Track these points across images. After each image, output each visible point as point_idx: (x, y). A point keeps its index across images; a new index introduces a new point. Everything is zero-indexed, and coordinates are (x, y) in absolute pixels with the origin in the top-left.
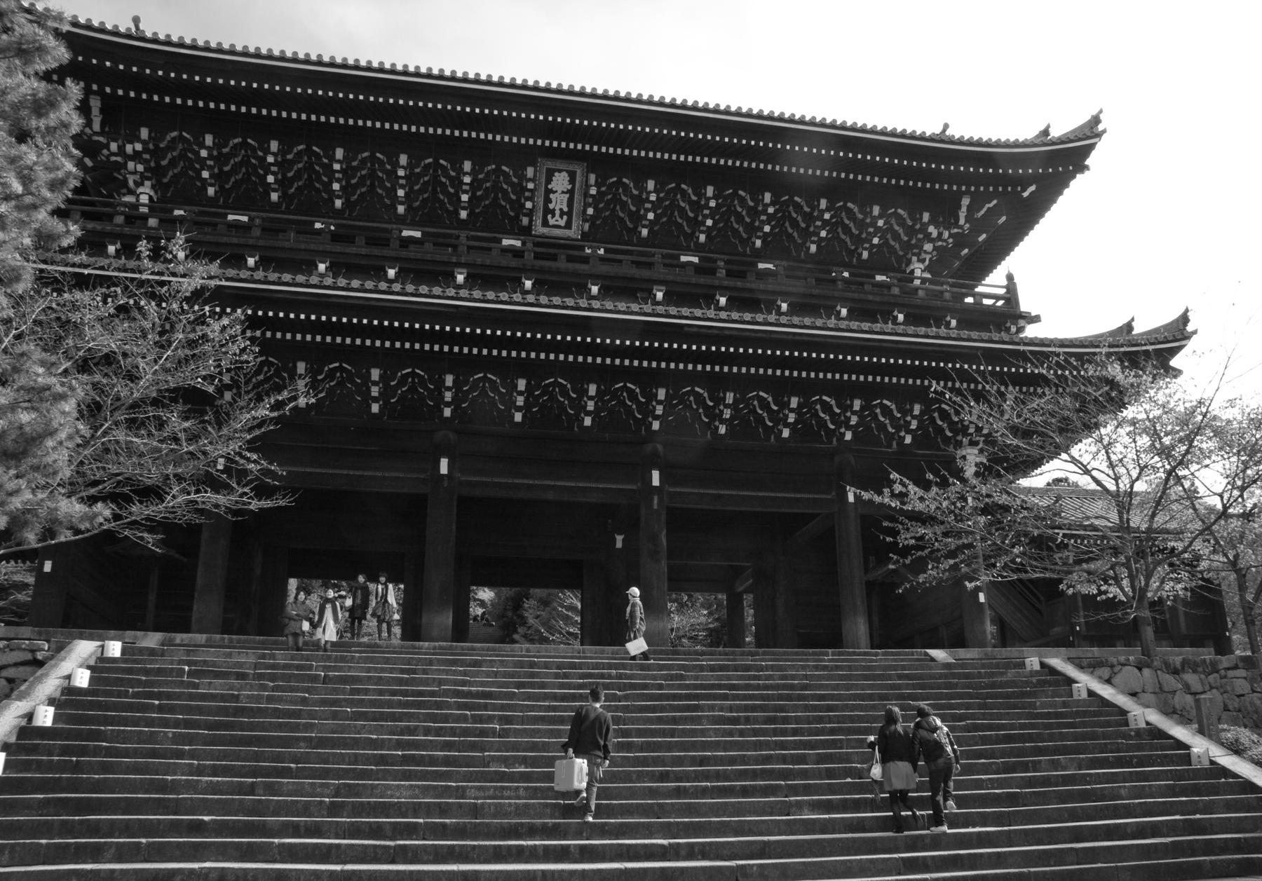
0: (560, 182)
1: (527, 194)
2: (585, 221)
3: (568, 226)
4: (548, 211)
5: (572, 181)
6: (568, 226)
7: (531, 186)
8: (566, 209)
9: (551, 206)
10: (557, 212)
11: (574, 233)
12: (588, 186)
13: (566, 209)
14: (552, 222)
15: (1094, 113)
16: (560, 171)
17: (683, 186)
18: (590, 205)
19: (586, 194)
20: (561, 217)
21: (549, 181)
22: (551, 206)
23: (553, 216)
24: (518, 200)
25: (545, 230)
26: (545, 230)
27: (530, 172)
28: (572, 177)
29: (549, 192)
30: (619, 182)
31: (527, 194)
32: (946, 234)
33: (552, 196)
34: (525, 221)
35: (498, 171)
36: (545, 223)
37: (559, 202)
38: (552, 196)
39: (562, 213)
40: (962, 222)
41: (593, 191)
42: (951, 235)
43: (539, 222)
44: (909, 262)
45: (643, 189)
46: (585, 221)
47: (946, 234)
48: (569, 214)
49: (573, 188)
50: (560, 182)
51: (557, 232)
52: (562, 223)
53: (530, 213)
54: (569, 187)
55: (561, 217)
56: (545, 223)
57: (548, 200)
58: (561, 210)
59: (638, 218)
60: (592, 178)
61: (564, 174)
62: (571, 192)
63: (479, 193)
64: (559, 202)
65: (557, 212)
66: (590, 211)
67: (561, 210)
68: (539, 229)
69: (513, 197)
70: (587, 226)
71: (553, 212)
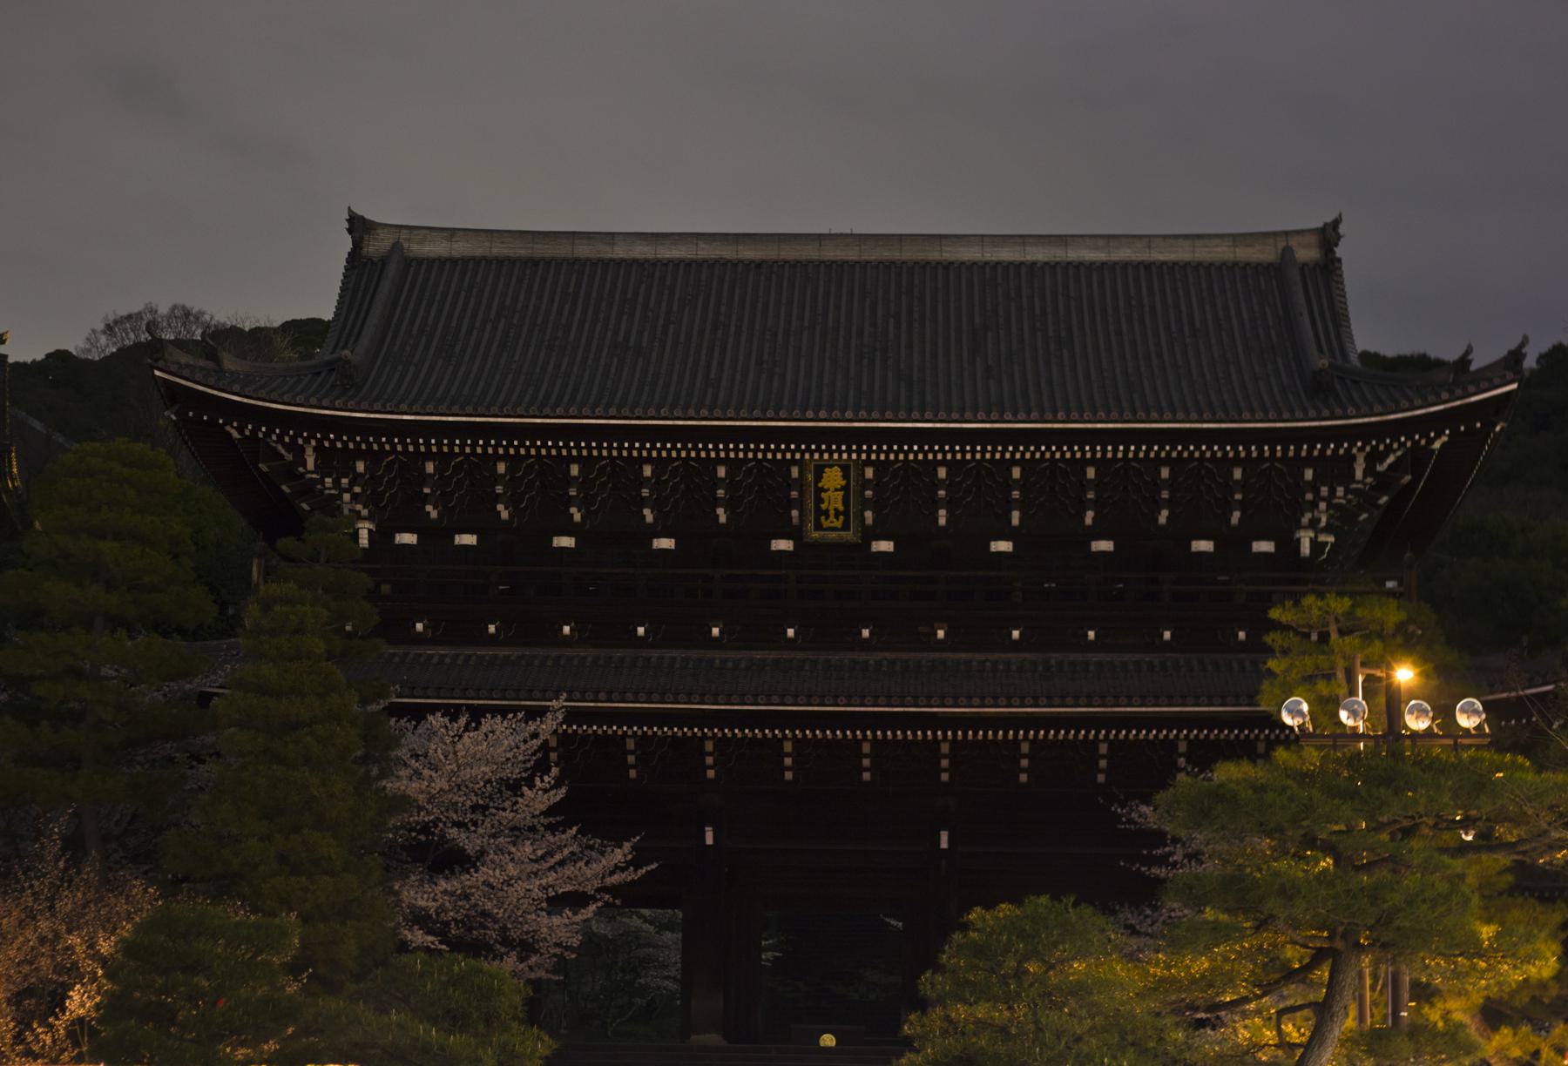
3: (846, 527)
4: (820, 513)
5: (846, 476)
8: (841, 508)
9: (824, 506)
10: (832, 512)
13: (841, 508)
14: (826, 524)
15: (1513, 346)
21: (818, 478)
22: (824, 506)
23: (827, 517)
26: (815, 535)
28: (845, 469)
29: (819, 491)
32: (1340, 491)
36: (818, 527)
37: (833, 500)
39: (837, 513)
40: (1359, 475)
42: (1347, 491)
43: (811, 526)
44: (1299, 527)
47: (1340, 491)
48: (846, 513)
49: (848, 484)
52: (838, 524)
55: (837, 517)
57: (819, 500)
62: (845, 489)
64: (833, 500)
65: (832, 512)
71: (826, 513)
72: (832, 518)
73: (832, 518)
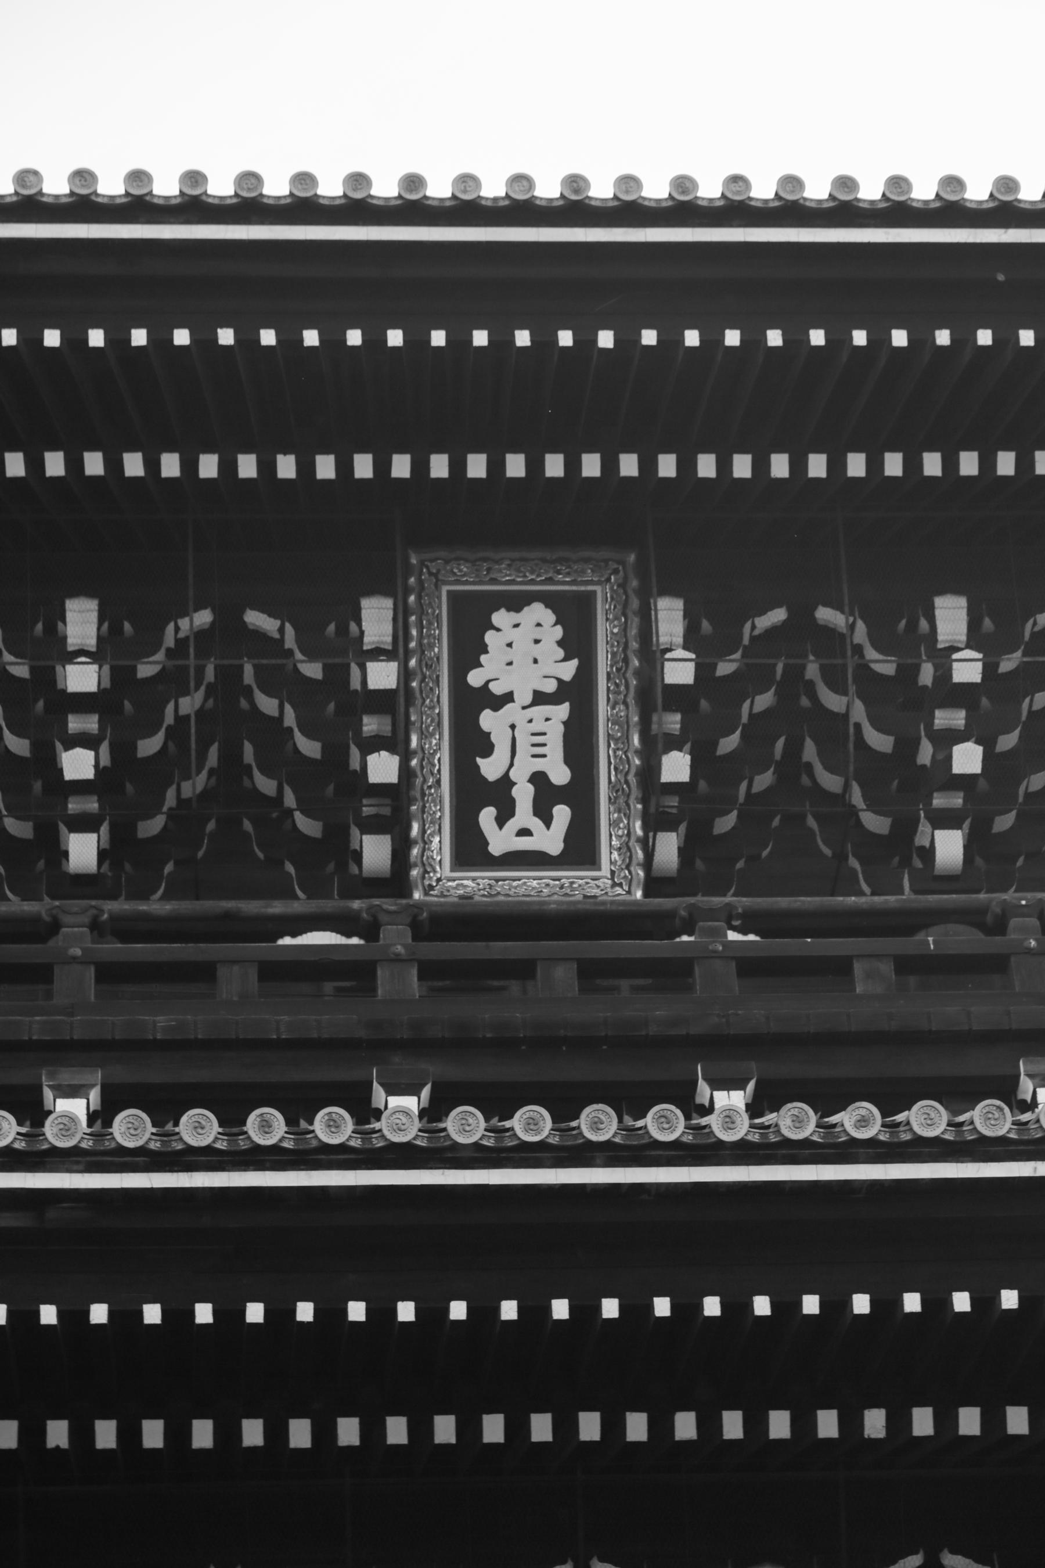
0: (523, 651)
1: (370, 725)
2: (656, 822)
3: (580, 849)
4: (477, 793)
5: (577, 642)
6: (580, 849)
7: (382, 676)
8: (560, 775)
9: (490, 768)
10: (523, 794)
11: (608, 880)
12: (652, 656)
13: (560, 775)
14: (500, 840)
16: (516, 603)
17: (825, 614)
18: (673, 743)
19: (650, 695)
20: (543, 813)
21: (468, 650)
22: (490, 768)
23: (506, 812)
24: (335, 757)
25: (474, 883)
27: (376, 620)
30: (803, 630)
31: (370, 725)
33: (488, 720)
34: (375, 852)
35: (229, 633)
36: (470, 850)
37: (525, 743)
38: (488, 720)
41: (680, 672)
43: (441, 846)
45: (918, 642)
46: (656, 822)
48: (580, 794)
49: (586, 675)
50: (523, 651)
51: (531, 885)
52: (550, 840)
53: (395, 808)
54: (568, 670)
55: (543, 813)
56: (470, 850)
57: (471, 743)
58: (539, 779)
59: (909, 785)
60: (670, 618)
61: (538, 613)
62: (577, 693)
63: (149, 746)
64: (525, 743)
65: (523, 794)
66: (676, 767)
67: (539, 779)
68: (445, 879)
69: (309, 747)
70: (668, 848)
72: (524, 813)
73: (524, 813)
